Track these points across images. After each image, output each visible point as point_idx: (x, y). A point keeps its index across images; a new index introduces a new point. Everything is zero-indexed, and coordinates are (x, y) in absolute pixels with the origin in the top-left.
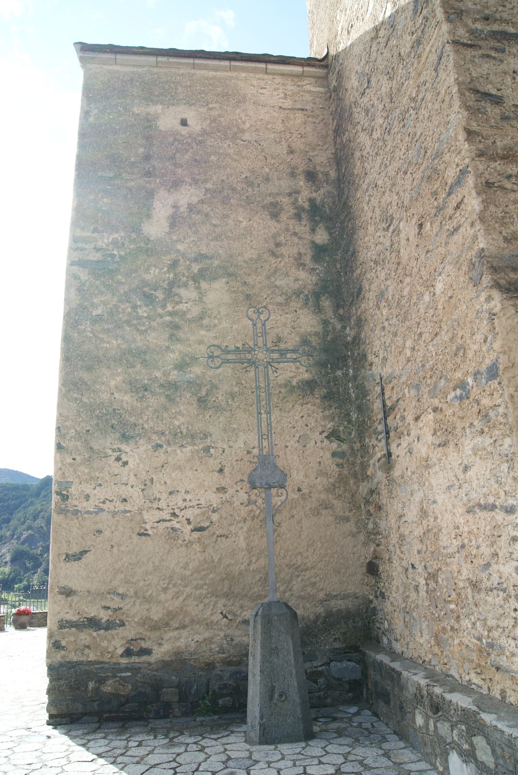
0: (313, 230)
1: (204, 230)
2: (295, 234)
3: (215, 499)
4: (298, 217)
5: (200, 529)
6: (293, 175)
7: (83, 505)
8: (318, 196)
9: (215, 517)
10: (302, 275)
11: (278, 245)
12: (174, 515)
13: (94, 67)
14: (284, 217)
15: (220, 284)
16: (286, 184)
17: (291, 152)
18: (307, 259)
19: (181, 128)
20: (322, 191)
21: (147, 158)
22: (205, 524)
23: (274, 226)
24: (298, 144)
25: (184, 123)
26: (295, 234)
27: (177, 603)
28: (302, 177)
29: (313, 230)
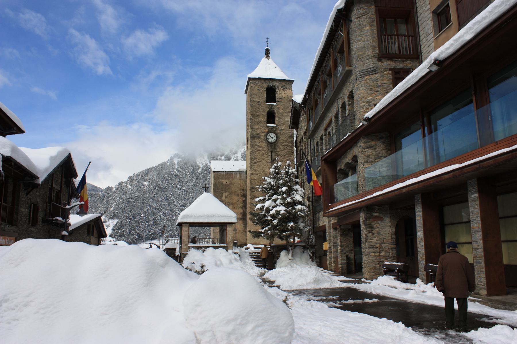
1: (229, 198)
4: (241, 196)
6: (241, 190)
7: (215, 232)
8: (244, 193)
10: (241, 204)
13: (215, 174)
15: (231, 206)
16: (240, 191)
17: (241, 186)
18: (242, 202)
21: (222, 188)
23: (238, 198)
24: (242, 185)
25: (227, 182)
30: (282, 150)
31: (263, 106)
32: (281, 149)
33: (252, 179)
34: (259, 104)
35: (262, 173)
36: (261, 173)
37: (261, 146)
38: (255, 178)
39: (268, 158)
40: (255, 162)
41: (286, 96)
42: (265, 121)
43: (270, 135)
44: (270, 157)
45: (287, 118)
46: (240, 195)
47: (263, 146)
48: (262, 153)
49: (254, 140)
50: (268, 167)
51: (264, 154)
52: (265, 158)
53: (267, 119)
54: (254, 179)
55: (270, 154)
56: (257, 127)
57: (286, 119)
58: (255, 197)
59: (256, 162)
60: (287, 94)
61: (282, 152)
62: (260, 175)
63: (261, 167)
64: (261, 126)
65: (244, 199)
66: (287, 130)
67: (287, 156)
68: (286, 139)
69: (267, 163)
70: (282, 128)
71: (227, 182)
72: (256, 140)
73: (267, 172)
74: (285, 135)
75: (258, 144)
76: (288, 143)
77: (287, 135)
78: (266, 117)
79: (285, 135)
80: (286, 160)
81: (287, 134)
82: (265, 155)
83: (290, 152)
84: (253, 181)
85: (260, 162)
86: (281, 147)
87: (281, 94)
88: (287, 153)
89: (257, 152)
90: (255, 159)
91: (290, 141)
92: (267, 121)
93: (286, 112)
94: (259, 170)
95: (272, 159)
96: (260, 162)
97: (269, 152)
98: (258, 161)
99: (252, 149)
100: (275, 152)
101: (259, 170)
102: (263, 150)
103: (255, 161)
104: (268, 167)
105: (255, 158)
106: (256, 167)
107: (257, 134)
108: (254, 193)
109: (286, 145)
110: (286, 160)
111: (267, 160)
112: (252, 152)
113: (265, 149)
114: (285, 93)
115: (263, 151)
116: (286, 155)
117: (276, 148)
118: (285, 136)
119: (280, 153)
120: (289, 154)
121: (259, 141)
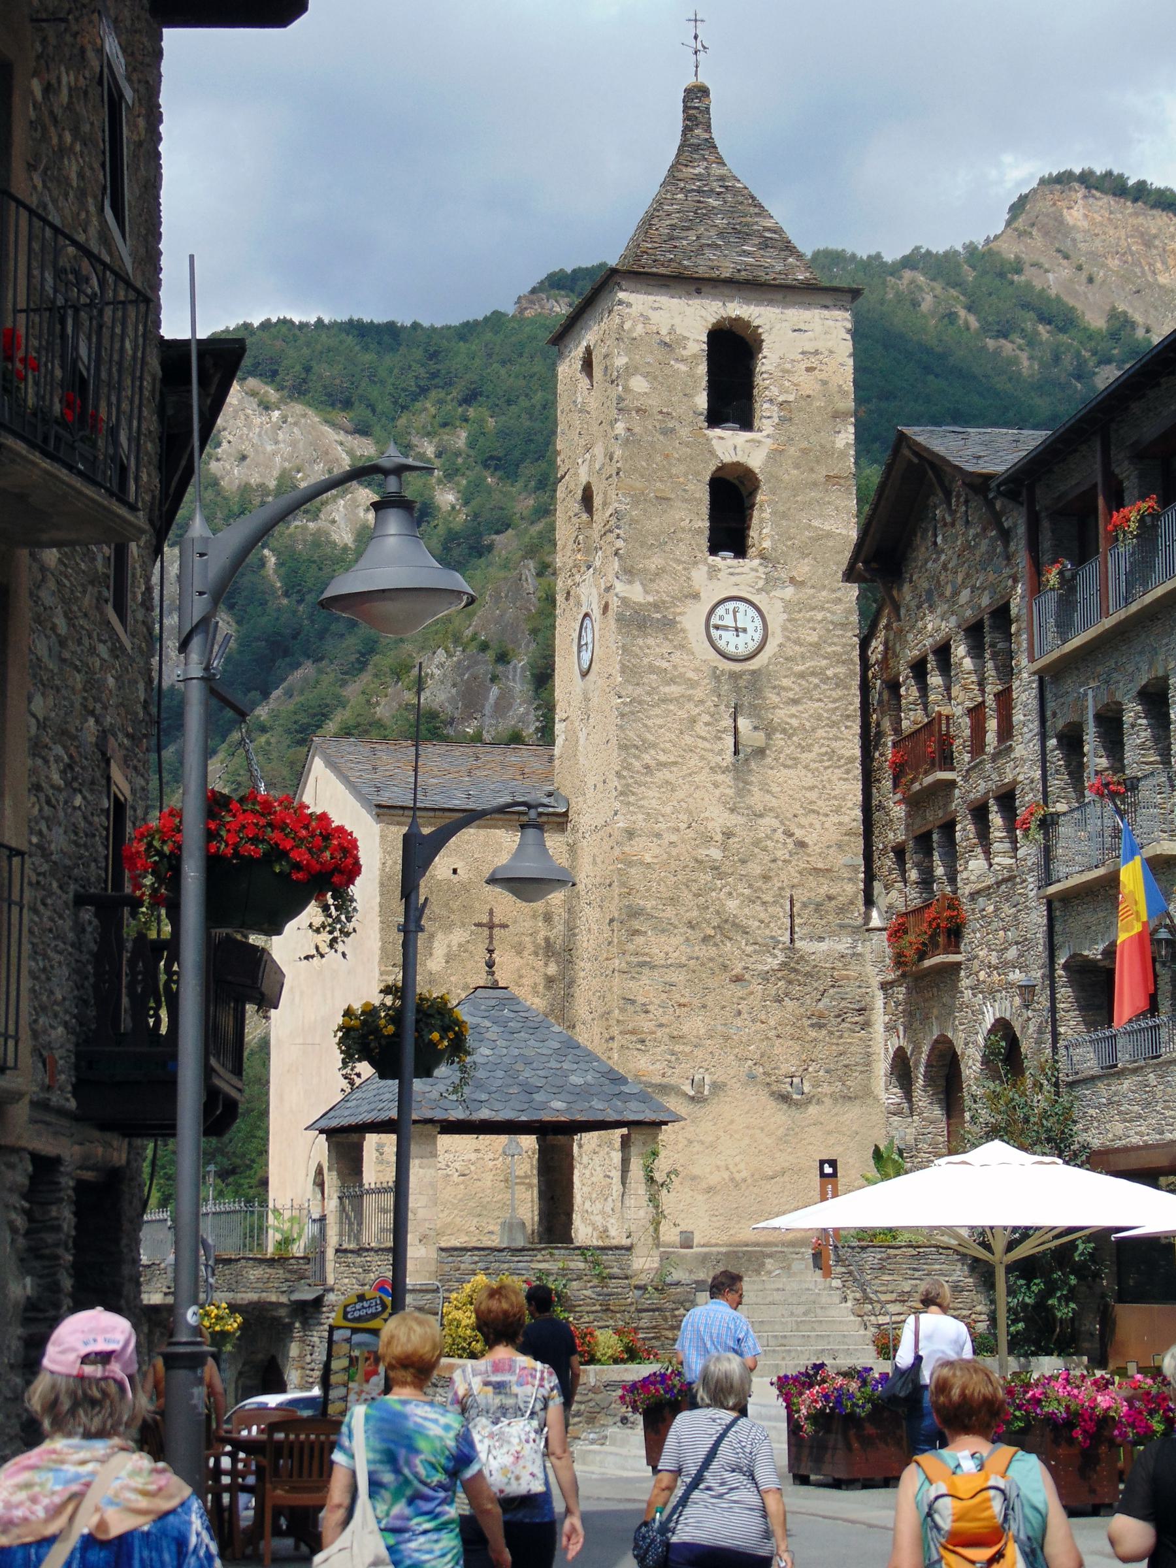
0: (546, 965)
2: (533, 968)
3: (473, 1156)
4: (536, 954)
5: (464, 1175)
9: (473, 1168)
11: (521, 977)
12: (448, 1166)
14: (526, 953)
18: (541, 988)
19: (453, 876)
20: (555, 931)
22: (467, 1172)
23: (518, 962)
25: (455, 871)
26: (533, 968)
27: (449, 1219)
28: (541, 918)
29: (546, 965)
30: (795, 702)
31: (687, 445)
32: (791, 695)
33: (630, 864)
34: (667, 432)
35: (683, 826)
36: (678, 830)
37: (681, 675)
38: (648, 859)
39: (718, 746)
40: (647, 767)
41: (818, 387)
42: (699, 531)
43: (735, 612)
44: (729, 741)
45: (821, 516)
46: (530, 948)
47: (691, 675)
48: (682, 714)
49: (640, 641)
50: (717, 792)
51: (693, 721)
52: (701, 744)
53: (713, 517)
54: (642, 863)
55: (729, 722)
56: (655, 562)
57: (815, 523)
58: (642, 965)
59: (653, 763)
60: (823, 376)
61: (793, 710)
62: (674, 838)
63: (680, 794)
64: (679, 562)
65: (552, 969)
66: (824, 587)
67: (821, 733)
68: (813, 638)
69: (711, 768)
70: (795, 574)
71: (455, 871)
72: (650, 641)
73: (710, 825)
74: (808, 615)
75: (665, 665)
76: (824, 662)
77: (820, 616)
78: (705, 510)
79: (808, 615)
80: (812, 755)
81: (823, 608)
82: (700, 729)
83: (837, 708)
84: (633, 871)
85: (675, 763)
86: (786, 682)
87: (788, 371)
88: (819, 718)
89: (657, 711)
90: (646, 750)
91: (838, 649)
92: (711, 529)
93: (815, 484)
94: (668, 810)
95: (736, 752)
96: (675, 763)
97: (723, 707)
98: (663, 758)
99: (630, 688)
100: (755, 711)
101: (668, 810)
102: (690, 698)
103: (647, 758)
104: (717, 792)
105: (644, 741)
106: (650, 794)
107: (656, 606)
108: (639, 940)
109: (813, 674)
110: (812, 755)
111: (709, 756)
112: (627, 709)
113: (698, 693)
114: (809, 369)
115: (691, 705)
116: (814, 730)
117: (760, 691)
118: (809, 620)
119: (781, 714)
120: (834, 724)
121: (666, 648)
